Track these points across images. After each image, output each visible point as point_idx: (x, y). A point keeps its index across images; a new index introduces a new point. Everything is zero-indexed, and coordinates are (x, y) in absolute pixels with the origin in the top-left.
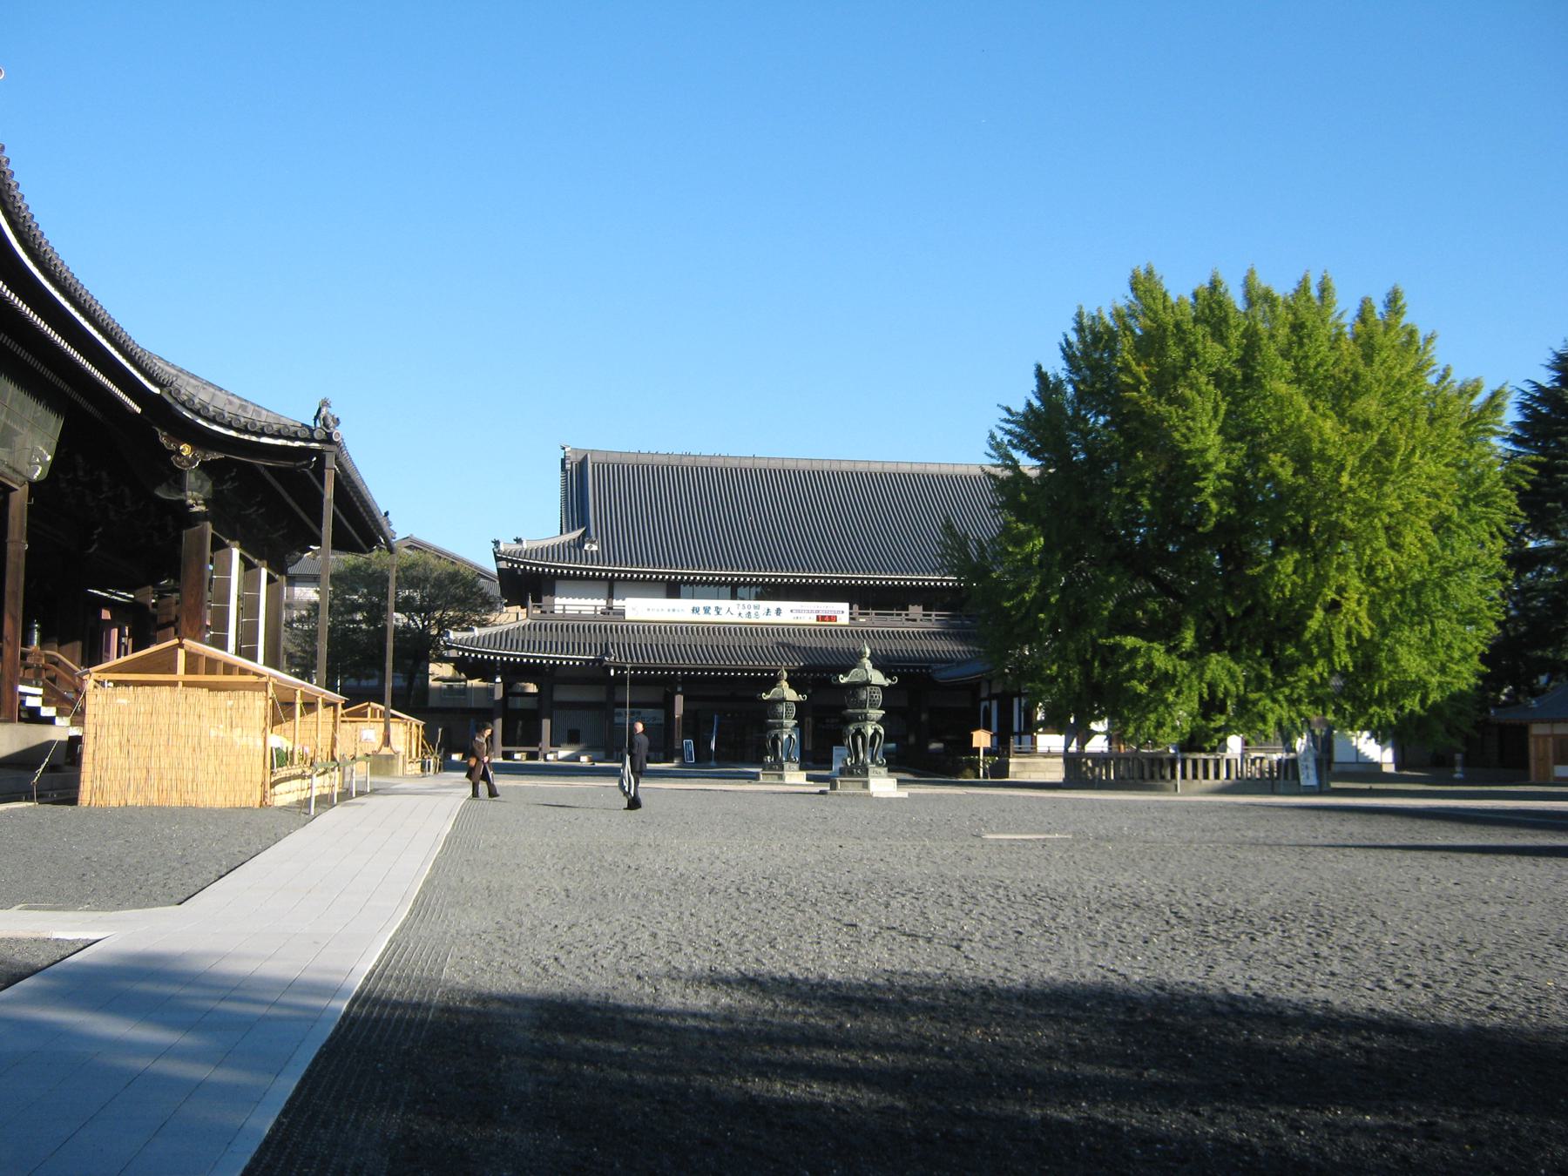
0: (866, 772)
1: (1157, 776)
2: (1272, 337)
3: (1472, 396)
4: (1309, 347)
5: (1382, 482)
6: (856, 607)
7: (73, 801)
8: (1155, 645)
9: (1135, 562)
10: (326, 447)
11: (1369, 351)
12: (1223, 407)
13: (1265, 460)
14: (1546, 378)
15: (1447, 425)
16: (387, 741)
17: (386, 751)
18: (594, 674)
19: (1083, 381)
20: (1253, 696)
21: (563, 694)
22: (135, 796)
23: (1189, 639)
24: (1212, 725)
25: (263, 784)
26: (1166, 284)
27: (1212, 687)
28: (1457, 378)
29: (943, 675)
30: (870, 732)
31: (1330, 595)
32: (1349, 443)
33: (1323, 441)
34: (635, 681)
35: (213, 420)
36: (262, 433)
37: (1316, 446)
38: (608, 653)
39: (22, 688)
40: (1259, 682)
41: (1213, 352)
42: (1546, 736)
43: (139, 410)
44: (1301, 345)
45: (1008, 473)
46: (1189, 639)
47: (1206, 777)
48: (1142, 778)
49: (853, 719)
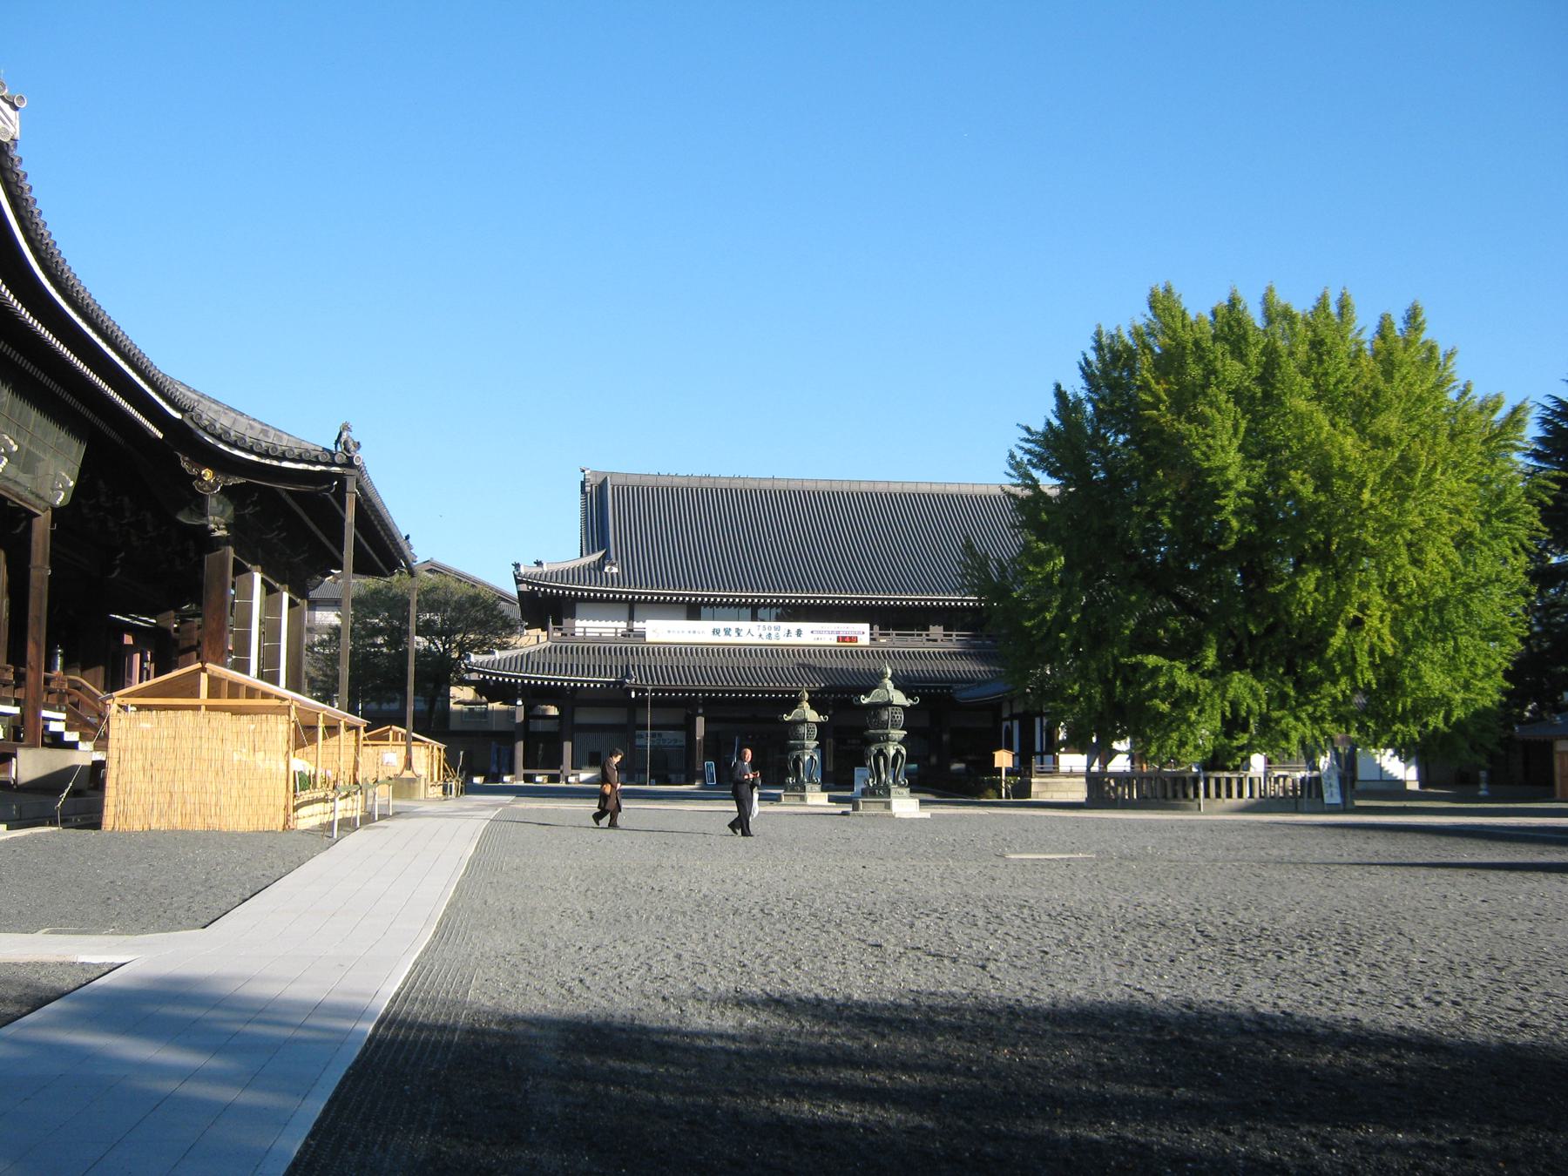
0: (888, 793)
1: (1180, 795)
2: (1291, 354)
3: (1493, 411)
4: (1329, 365)
5: (1403, 499)
6: (876, 627)
7: (96, 825)
8: (1177, 663)
9: (1155, 580)
10: (347, 471)
11: (1388, 366)
12: (1243, 424)
13: (1286, 477)
15: (1468, 441)
16: (408, 764)
17: (408, 774)
18: (615, 696)
19: (1103, 399)
20: (1276, 714)
21: (583, 717)
22: (158, 820)
23: (1210, 657)
24: (1235, 743)
25: (286, 807)
26: (1185, 303)
27: (1234, 705)
28: (1478, 393)
29: (963, 695)
30: (892, 752)
31: (1353, 612)
32: (1370, 460)
33: (1344, 458)
34: (656, 703)
35: (234, 445)
36: (283, 458)
37: (1337, 463)
38: (628, 676)
39: (45, 713)
40: (1282, 700)
41: (1233, 370)
43: (160, 436)
44: (1321, 362)
45: (1028, 492)
46: (1210, 657)
47: (1229, 796)
48: (1165, 797)
49: (876, 739)
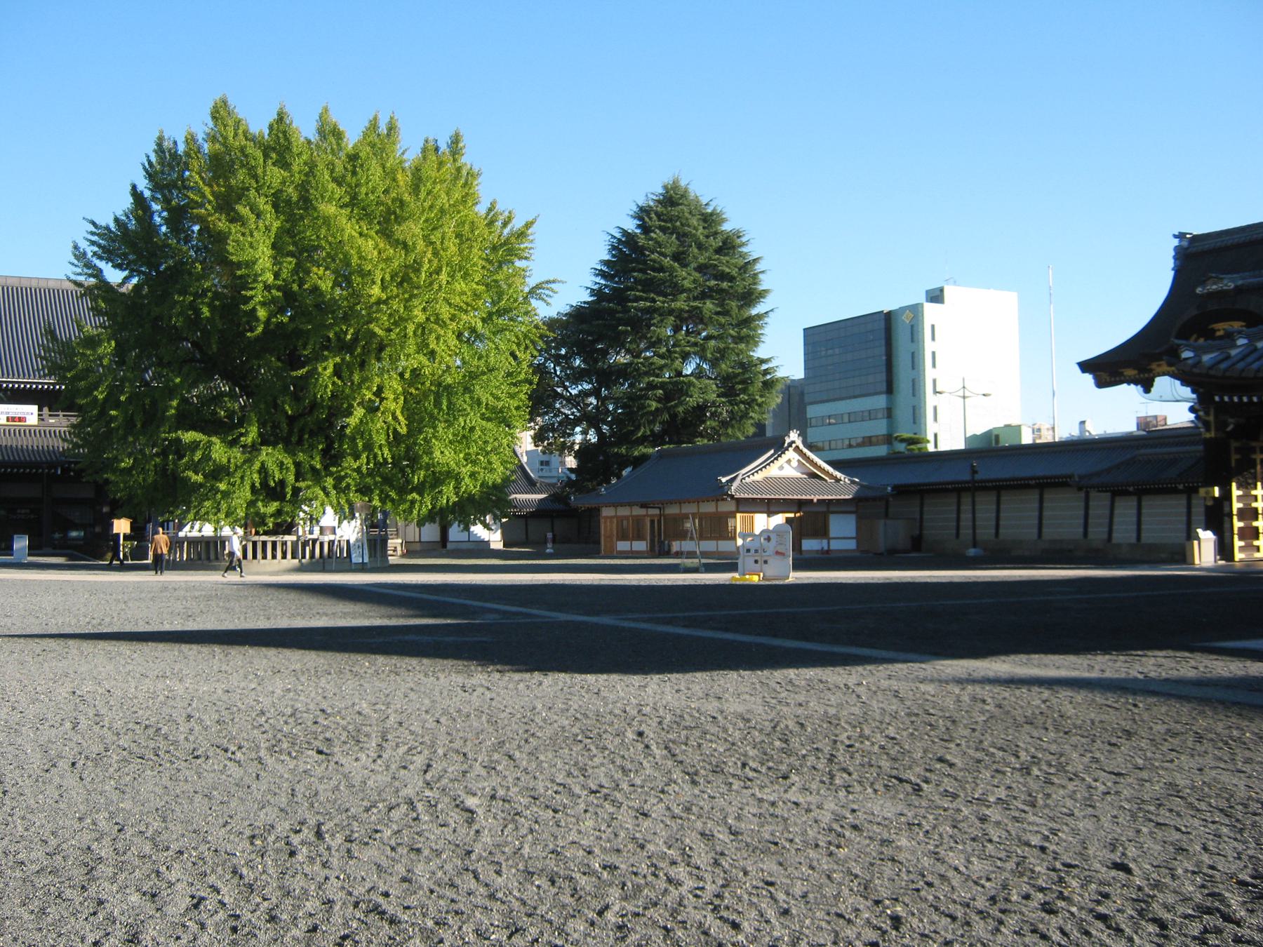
6: (46, 410)
8: (214, 439)
12: (276, 224)
14: (631, 225)
15: (471, 247)
23: (252, 434)
37: (355, 261)
41: (275, 175)
42: (612, 517)
44: (354, 173)
45: (93, 281)
46: (252, 434)
47: (284, 557)
48: (208, 559)
